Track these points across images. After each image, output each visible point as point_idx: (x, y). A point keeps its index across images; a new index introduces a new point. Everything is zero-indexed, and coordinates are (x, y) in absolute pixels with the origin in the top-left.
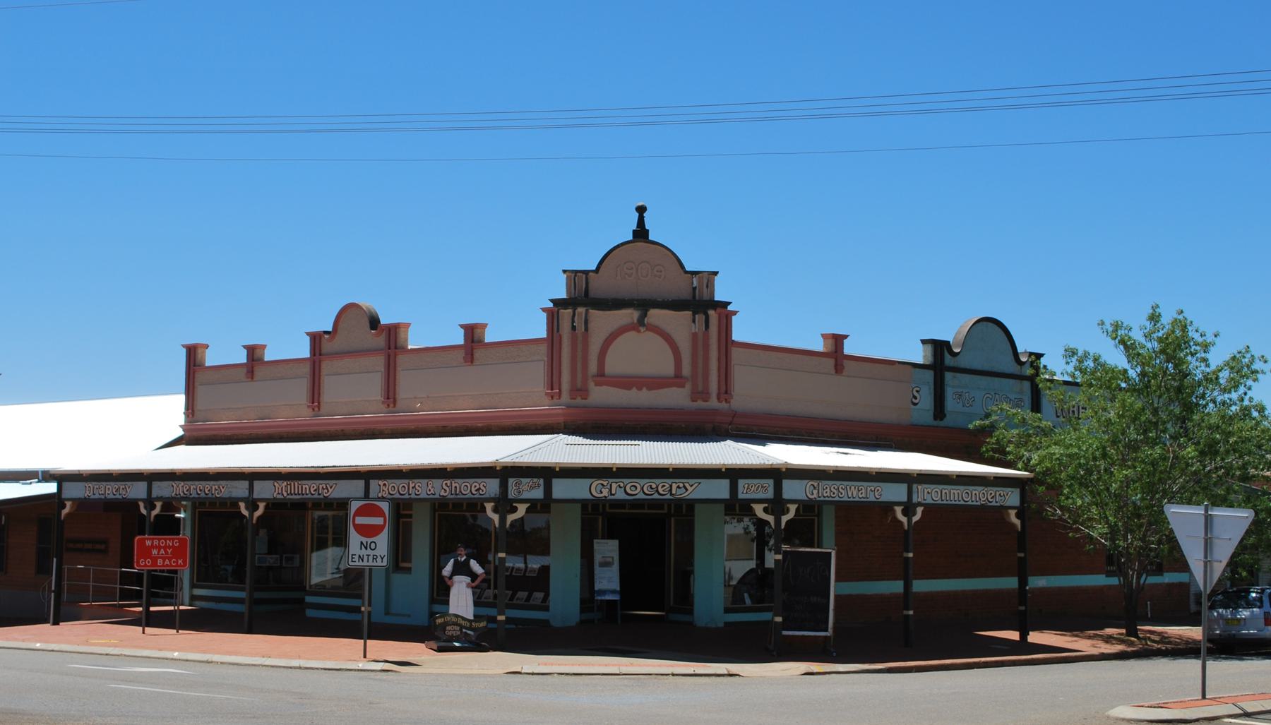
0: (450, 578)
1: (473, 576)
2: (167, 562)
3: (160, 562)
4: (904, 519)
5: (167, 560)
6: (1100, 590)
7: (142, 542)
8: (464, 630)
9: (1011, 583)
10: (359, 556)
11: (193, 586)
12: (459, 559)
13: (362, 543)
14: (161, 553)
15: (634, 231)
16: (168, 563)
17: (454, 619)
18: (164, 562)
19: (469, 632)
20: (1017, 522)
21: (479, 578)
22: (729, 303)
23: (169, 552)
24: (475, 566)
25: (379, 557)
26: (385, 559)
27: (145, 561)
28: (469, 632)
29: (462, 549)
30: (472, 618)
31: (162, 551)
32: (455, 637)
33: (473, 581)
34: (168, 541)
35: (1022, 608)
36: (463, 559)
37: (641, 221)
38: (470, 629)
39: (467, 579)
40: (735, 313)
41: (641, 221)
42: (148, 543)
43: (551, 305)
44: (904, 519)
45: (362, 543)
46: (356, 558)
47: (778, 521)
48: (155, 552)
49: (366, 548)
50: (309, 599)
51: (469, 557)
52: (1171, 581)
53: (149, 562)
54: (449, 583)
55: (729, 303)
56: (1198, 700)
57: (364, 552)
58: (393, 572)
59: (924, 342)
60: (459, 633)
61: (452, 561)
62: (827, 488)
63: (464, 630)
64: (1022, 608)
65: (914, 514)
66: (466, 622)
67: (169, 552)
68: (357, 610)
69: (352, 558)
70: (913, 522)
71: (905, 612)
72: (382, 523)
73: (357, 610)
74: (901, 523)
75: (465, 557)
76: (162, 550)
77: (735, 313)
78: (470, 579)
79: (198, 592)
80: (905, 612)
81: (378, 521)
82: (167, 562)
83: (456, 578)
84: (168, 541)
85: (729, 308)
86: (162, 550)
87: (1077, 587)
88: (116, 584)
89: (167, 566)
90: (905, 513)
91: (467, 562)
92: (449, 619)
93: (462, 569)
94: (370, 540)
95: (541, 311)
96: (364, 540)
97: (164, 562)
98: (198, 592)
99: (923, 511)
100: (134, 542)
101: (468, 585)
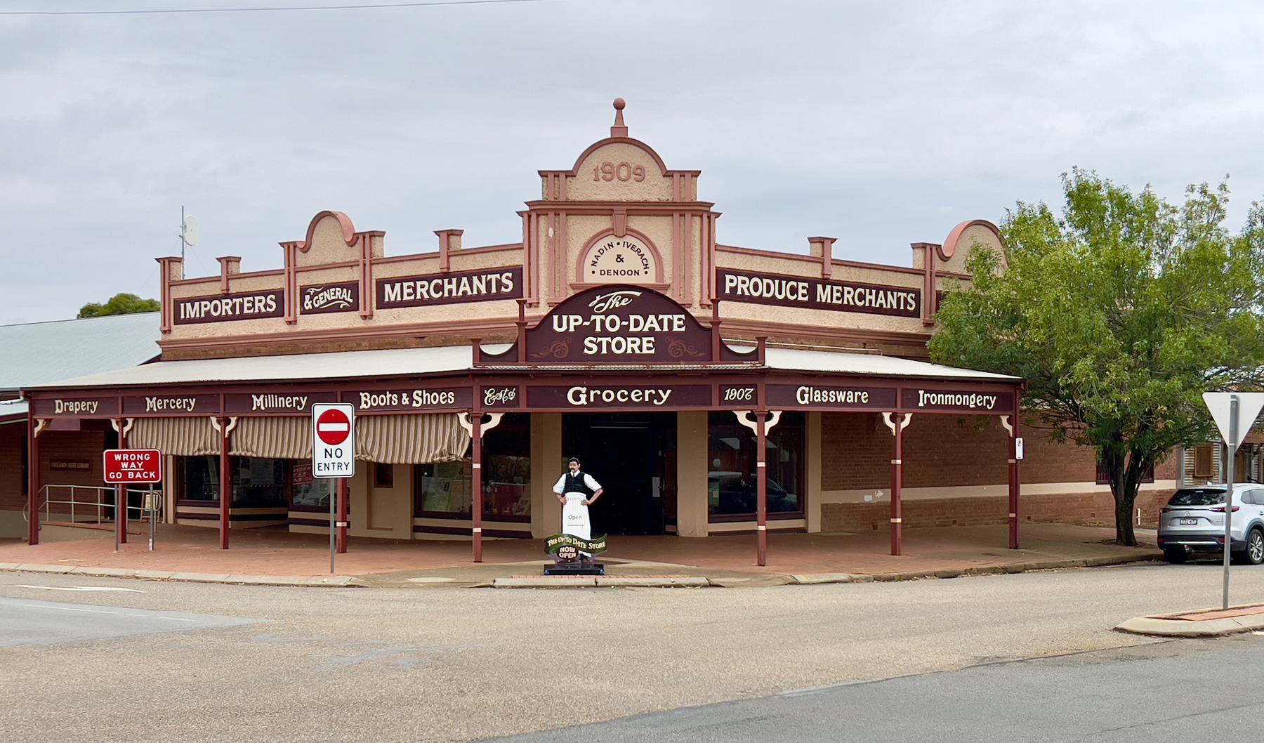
0: (563, 495)
1: (589, 493)
2: (138, 475)
3: (131, 475)
4: (892, 425)
5: (138, 473)
6: (1090, 497)
7: (110, 456)
8: (580, 552)
9: (1003, 491)
10: (325, 465)
11: (176, 504)
12: (572, 473)
13: (326, 450)
14: (131, 466)
15: (612, 128)
16: (141, 477)
17: (569, 540)
18: (135, 475)
19: (585, 554)
20: (1009, 428)
21: (595, 494)
22: (713, 204)
23: (140, 465)
24: (589, 481)
25: (343, 464)
26: (350, 466)
27: (115, 475)
28: (585, 554)
29: (575, 463)
30: (589, 538)
31: (133, 465)
32: (570, 559)
33: (589, 498)
34: (138, 455)
35: (1013, 515)
36: (576, 474)
37: (619, 118)
38: (587, 550)
39: (583, 496)
40: (718, 215)
41: (619, 118)
42: (118, 457)
43: (527, 208)
44: (892, 425)
45: (326, 450)
46: (323, 468)
47: (761, 428)
48: (124, 465)
49: (331, 456)
50: (291, 515)
51: (584, 469)
52: (1162, 489)
53: (119, 475)
54: (562, 500)
55: (713, 204)
56: (1219, 611)
57: (328, 460)
58: (375, 487)
59: (914, 246)
60: (574, 555)
61: (564, 476)
62: (850, 394)
63: (580, 552)
64: (1013, 515)
65: (903, 419)
66: (582, 543)
67: (140, 465)
68: (469, 532)
69: (319, 467)
70: (902, 428)
71: (893, 520)
72: (346, 430)
73: (327, 523)
74: (890, 429)
75: (578, 472)
76: (133, 463)
77: (718, 215)
78: (585, 495)
79: (181, 509)
80: (893, 520)
81: (342, 427)
82: (138, 475)
83: (568, 495)
84: (138, 455)
85: (712, 209)
86: (133, 463)
87: (1067, 495)
88: (71, 501)
89: (138, 479)
90: (893, 418)
91: (581, 478)
92: (562, 539)
93: (575, 485)
94: (334, 447)
95: (712, 202)
96: (329, 447)
97: (135, 475)
98: (181, 509)
99: (911, 417)
100: (102, 456)
101: (583, 503)
